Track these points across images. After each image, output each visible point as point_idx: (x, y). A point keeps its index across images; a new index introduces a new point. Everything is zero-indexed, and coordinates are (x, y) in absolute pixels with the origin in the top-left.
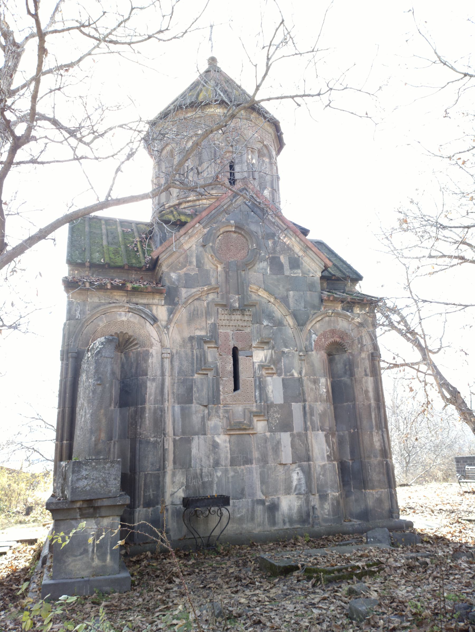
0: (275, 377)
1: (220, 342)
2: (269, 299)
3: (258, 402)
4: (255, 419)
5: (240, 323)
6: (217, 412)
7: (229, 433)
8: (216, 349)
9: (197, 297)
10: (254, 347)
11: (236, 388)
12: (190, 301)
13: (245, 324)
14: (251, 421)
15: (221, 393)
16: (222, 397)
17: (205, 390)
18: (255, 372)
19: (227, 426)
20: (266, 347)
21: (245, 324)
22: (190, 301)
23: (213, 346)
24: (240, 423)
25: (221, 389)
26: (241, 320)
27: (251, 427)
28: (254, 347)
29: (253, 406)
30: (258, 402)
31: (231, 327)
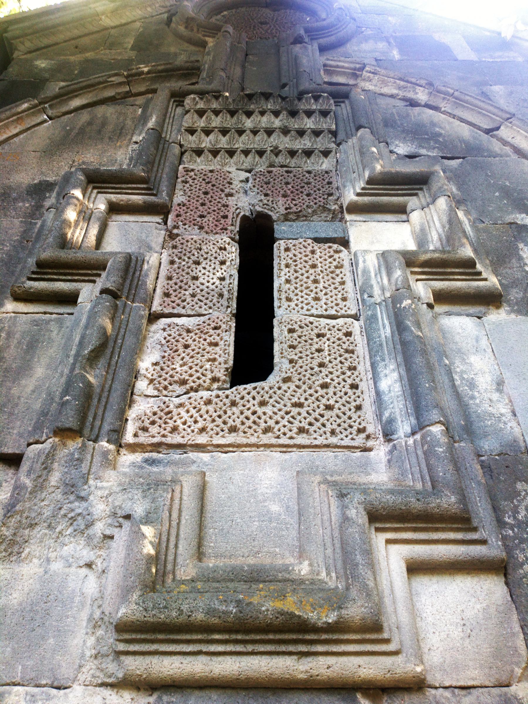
0: (497, 317)
1: (179, 198)
2: (410, 95)
3: (403, 427)
4: (392, 557)
5: (285, 143)
6: (74, 489)
7: (136, 665)
8: (158, 219)
9: (110, 93)
10: (355, 209)
11: (252, 360)
12: (76, 103)
13: (306, 143)
14: (353, 562)
15: (142, 385)
16: (141, 407)
17: (40, 371)
18: (365, 290)
19: (125, 594)
20: (412, 202)
21: (306, 143)
22: (76, 103)
23: (137, 199)
24: (255, 577)
25: (145, 364)
26: (285, 131)
27: (356, 611)
28: (355, 209)
29: (365, 467)
30: (403, 427)
31: (239, 157)
